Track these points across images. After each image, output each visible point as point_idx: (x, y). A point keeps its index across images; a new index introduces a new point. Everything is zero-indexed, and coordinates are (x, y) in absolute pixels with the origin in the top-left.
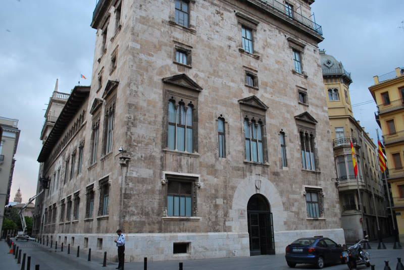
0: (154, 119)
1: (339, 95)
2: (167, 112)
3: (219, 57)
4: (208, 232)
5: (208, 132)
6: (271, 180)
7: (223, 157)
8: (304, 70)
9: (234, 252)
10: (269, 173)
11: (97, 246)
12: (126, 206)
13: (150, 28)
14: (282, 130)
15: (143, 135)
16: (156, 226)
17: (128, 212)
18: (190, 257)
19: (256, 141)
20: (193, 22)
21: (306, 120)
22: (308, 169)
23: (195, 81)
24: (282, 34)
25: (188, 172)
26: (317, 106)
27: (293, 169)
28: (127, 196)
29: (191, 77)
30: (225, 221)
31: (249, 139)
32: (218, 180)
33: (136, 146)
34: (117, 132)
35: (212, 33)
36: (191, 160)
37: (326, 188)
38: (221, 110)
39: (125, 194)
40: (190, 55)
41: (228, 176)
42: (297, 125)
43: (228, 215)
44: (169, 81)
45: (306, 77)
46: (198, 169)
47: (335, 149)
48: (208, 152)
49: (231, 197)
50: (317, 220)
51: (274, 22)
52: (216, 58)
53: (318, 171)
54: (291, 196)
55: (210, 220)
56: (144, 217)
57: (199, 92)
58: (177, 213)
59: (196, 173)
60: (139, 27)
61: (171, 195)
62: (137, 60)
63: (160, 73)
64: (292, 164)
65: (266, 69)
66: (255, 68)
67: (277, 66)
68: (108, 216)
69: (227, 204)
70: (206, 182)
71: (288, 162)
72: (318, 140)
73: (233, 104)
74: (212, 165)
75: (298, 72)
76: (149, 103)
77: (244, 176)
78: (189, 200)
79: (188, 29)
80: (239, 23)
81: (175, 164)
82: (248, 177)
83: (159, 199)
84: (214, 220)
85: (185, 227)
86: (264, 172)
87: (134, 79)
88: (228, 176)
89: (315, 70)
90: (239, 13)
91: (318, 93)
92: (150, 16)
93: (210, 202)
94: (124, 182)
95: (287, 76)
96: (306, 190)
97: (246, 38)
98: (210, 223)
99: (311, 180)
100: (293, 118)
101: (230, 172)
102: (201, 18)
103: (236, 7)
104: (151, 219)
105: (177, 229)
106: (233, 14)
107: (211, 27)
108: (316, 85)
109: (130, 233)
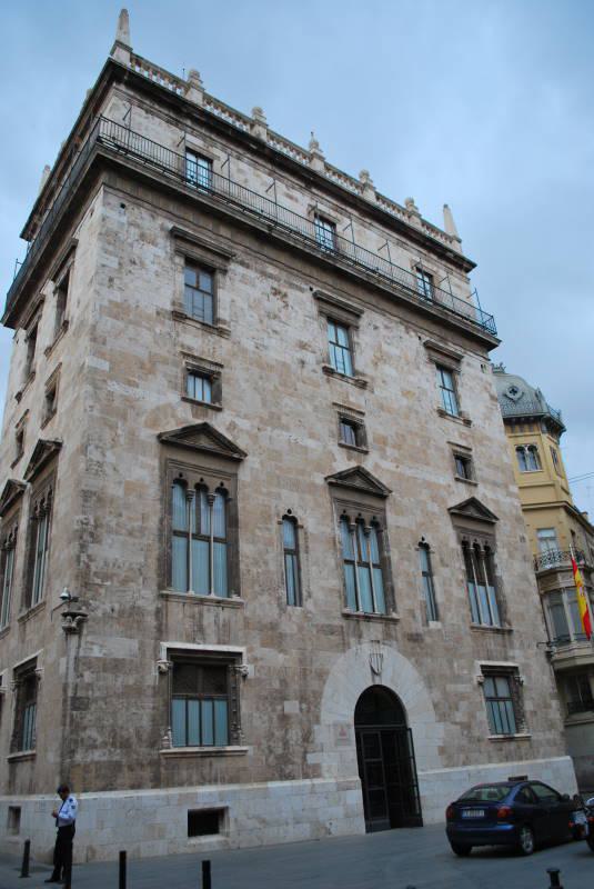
1: (538, 457)
2: (168, 509)
3: (281, 384)
5: (260, 549)
6: (405, 653)
7: (295, 604)
8: (462, 409)
9: (328, 826)
10: (399, 636)
11: (8, 827)
12: (77, 727)
13: (131, 327)
14: (423, 539)
15: (116, 560)
16: (147, 773)
17: (82, 740)
18: (226, 843)
19: (367, 565)
20: (223, 313)
21: (472, 515)
22: (484, 625)
23: (230, 438)
24: (413, 334)
25: (219, 643)
26: (495, 484)
27: (453, 625)
28: (78, 703)
29: (221, 430)
30: (305, 752)
31: (351, 562)
32: (287, 657)
33: (100, 586)
34: (57, 554)
35: (265, 336)
36: (225, 614)
37: (527, 666)
38: (290, 500)
39: (75, 698)
40: (217, 383)
41: (310, 648)
42: (456, 527)
43: (311, 739)
44: (174, 440)
45: (468, 423)
46: (241, 634)
47: (539, 577)
48: (261, 595)
49: (318, 695)
50: (512, 739)
51: (394, 310)
52: (276, 388)
53: (507, 627)
54: (451, 687)
55: (271, 752)
56: (118, 751)
57: (238, 461)
58: (194, 738)
59: (237, 644)
60: (108, 324)
61: (179, 698)
62: (102, 395)
63: (154, 423)
64: (449, 615)
65: (382, 407)
67: (405, 402)
68: (34, 752)
69: (308, 712)
70: (260, 663)
72: (500, 557)
73: (313, 485)
75: (450, 413)
76: (130, 488)
77: (345, 646)
78: (221, 706)
79: (214, 327)
80: (321, 313)
81: (188, 624)
83: (154, 708)
84: (279, 751)
85: (213, 772)
86: (388, 636)
87: (96, 436)
88: (310, 648)
89: (487, 407)
90: (322, 294)
91: (495, 456)
92: (132, 303)
93: (270, 709)
94: (71, 671)
95: (426, 422)
96: (483, 672)
98: (271, 758)
99: (492, 647)
101: (314, 639)
102: (240, 303)
103: (314, 281)
104: (135, 756)
105: (195, 778)
106: (308, 296)
107: (261, 321)
108: (489, 439)
109: (85, 791)
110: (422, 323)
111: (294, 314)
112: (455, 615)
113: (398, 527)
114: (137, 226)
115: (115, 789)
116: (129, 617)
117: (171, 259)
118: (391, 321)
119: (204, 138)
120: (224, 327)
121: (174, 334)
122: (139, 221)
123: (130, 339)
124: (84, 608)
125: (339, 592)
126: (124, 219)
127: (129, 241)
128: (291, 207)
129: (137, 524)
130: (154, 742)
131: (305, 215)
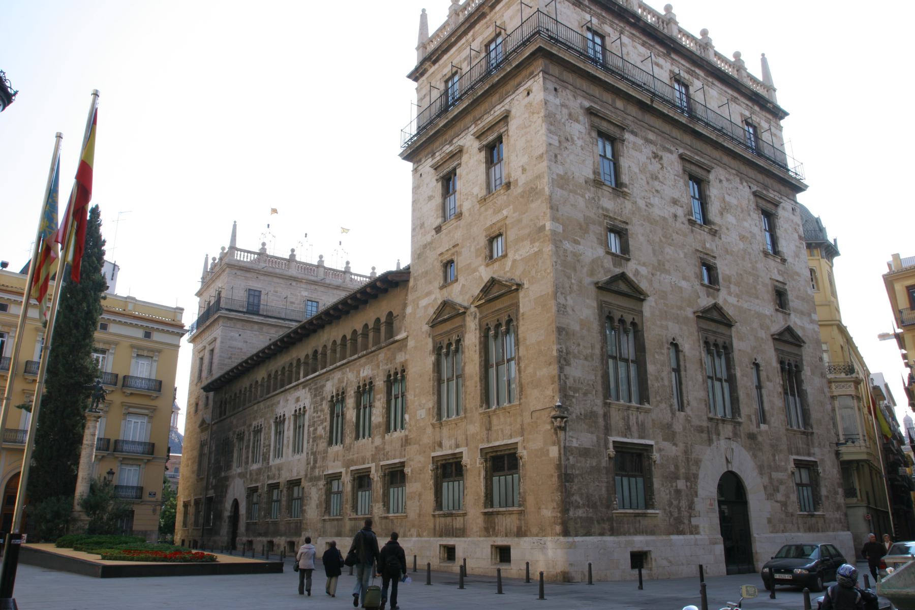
0: (590, 351)
4: (670, 534)
5: (658, 366)
6: (745, 447)
10: (742, 435)
16: (606, 526)
19: (720, 380)
20: (625, 179)
21: (788, 339)
22: (795, 428)
24: (745, 184)
26: (802, 313)
29: (630, 275)
30: (690, 516)
31: (711, 378)
33: (573, 397)
34: (530, 370)
37: (822, 460)
38: (674, 330)
42: (776, 350)
45: (784, 261)
46: (651, 431)
48: (660, 402)
49: (696, 476)
50: (813, 516)
53: (810, 430)
54: (775, 475)
59: (649, 439)
61: (617, 475)
64: (773, 420)
65: (727, 251)
66: (712, 251)
67: (741, 245)
69: (691, 488)
70: (663, 453)
71: (767, 415)
77: (710, 441)
78: (640, 480)
79: (619, 188)
80: (684, 171)
81: (621, 424)
84: (676, 515)
86: (735, 434)
89: (797, 246)
91: (802, 288)
92: (569, 174)
94: (562, 456)
95: (756, 262)
97: (694, 197)
98: (672, 520)
100: (770, 338)
105: (632, 531)
106: (674, 158)
107: (648, 183)
108: (798, 274)
109: (576, 536)
110: (752, 173)
112: (777, 420)
115: (590, 535)
116: (590, 417)
117: (589, 134)
118: (730, 174)
119: (598, 16)
120: (625, 189)
122: (567, 102)
123: (572, 205)
126: (558, 101)
127: (563, 120)
130: (609, 506)
131: (667, 82)
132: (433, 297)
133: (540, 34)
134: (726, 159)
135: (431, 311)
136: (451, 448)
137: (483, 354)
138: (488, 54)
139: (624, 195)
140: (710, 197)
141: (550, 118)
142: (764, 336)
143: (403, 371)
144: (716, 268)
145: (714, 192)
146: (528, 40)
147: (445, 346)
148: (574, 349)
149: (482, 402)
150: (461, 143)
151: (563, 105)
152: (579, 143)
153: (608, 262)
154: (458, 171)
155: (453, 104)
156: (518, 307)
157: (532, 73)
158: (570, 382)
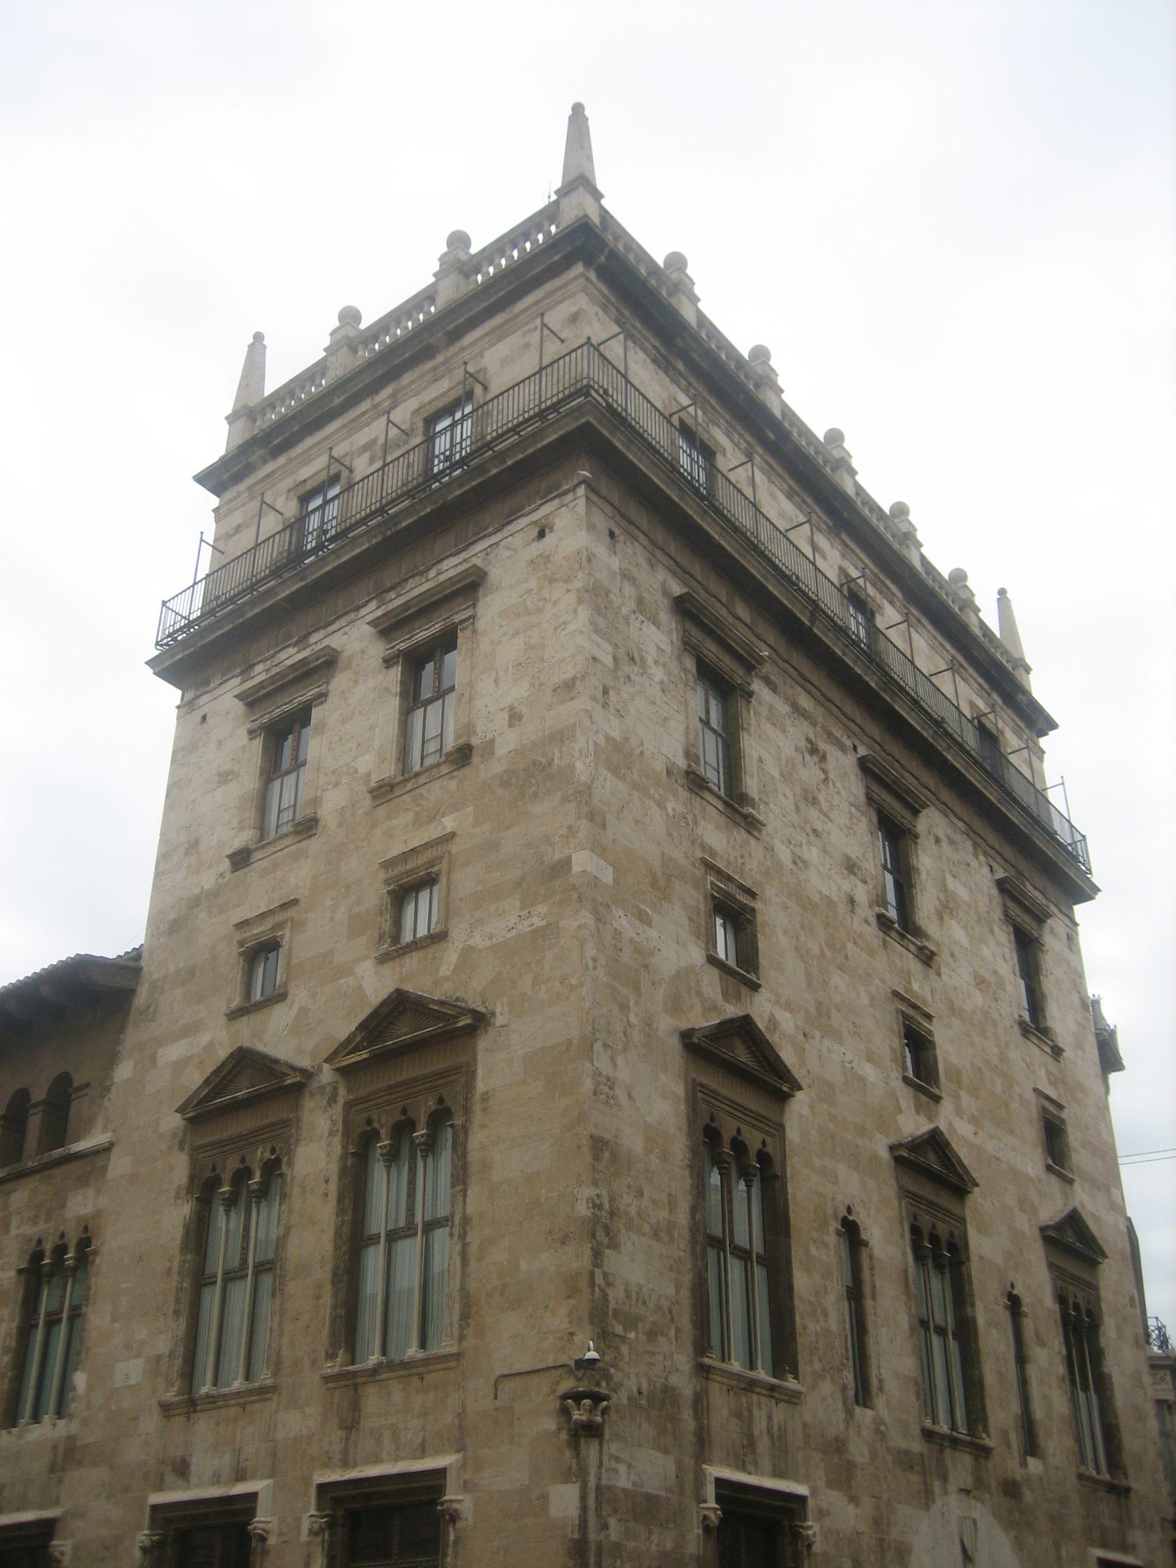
0: (663, 1214)
2: (700, 1189)
5: (816, 1279)
10: (993, 1483)
13: (635, 793)
15: (640, 1287)
20: (751, 785)
24: (982, 858)
25: (778, 1474)
33: (623, 1339)
36: (780, 1413)
41: (885, 1496)
42: (1052, 1266)
45: (1057, 1052)
46: (800, 1456)
53: (1124, 1482)
57: (782, 1098)
60: (608, 787)
65: (952, 1007)
66: (925, 1001)
67: (978, 999)
70: (827, 1522)
71: (1041, 1432)
73: (874, 1158)
74: (836, 1439)
77: (926, 1497)
79: (738, 807)
80: (870, 799)
82: (939, 1503)
86: (980, 1482)
95: (1007, 1044)
100: (1037, 1235)
107: (797, 808)
111: (836, 797)
112: (1057, 1445)
113: (981, 1258)
114: (633, 581)
121: (690, 817)
122: (634, 570)
123: (637, 822)
124: (604, 1384)
125: (916, 1384)
126: (615, 563)
128: (823, 563)
129: (663, 1214)
132: (204, 1038)
133: (587, 395)
134: (946, 795)
135: (194, 1078)
136: (216, 1480)
137: (347, 1203)
138: (430, 439)
139: (751, 825)
140: (918, 871)
141: (596, 596)
142: (1026, 1229)
143: (84, 1243)
144: (932, 1043)
145: (925, 860)
146: (555, 407)
147: (227, 1177)
148: (628, 1202)
149: (334, 1344)
150: (335, 641)
151: (626, 576)
152: (658, 674)
153: (711, 983)
154: (316, 713)
155: (314, 551)
156: (473, 1074)
157: (558, 486)
158: (616, 1296)
